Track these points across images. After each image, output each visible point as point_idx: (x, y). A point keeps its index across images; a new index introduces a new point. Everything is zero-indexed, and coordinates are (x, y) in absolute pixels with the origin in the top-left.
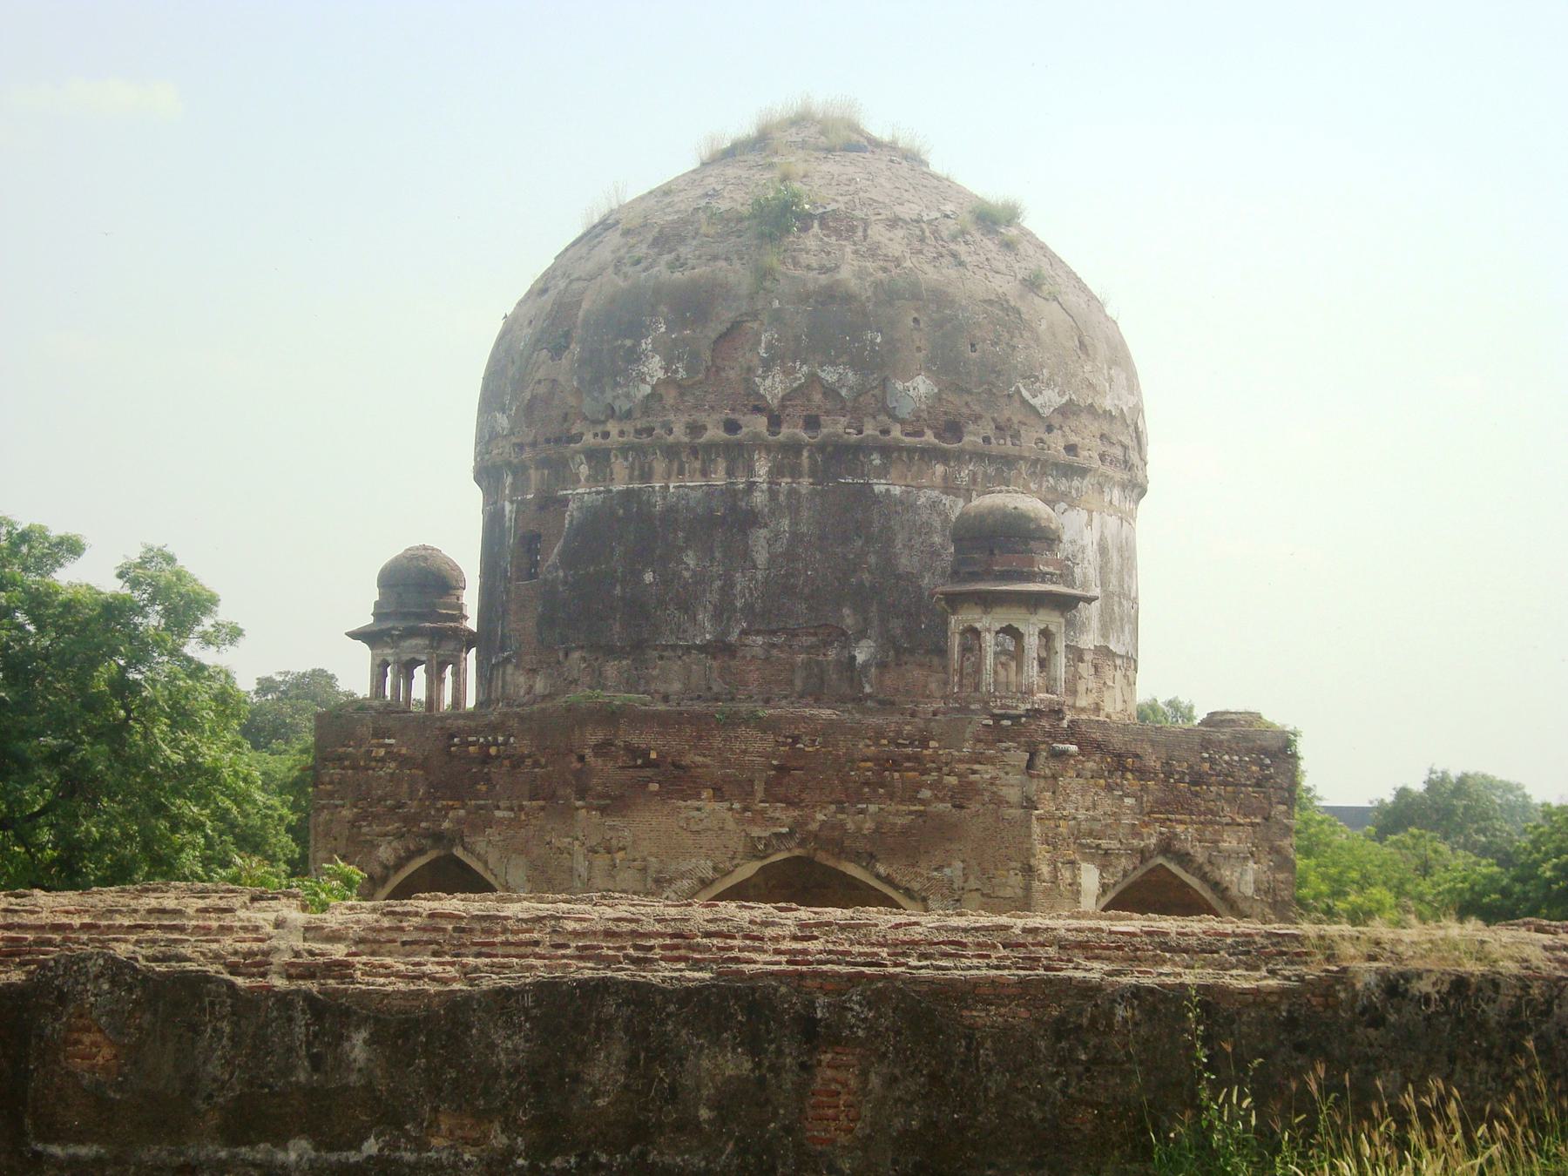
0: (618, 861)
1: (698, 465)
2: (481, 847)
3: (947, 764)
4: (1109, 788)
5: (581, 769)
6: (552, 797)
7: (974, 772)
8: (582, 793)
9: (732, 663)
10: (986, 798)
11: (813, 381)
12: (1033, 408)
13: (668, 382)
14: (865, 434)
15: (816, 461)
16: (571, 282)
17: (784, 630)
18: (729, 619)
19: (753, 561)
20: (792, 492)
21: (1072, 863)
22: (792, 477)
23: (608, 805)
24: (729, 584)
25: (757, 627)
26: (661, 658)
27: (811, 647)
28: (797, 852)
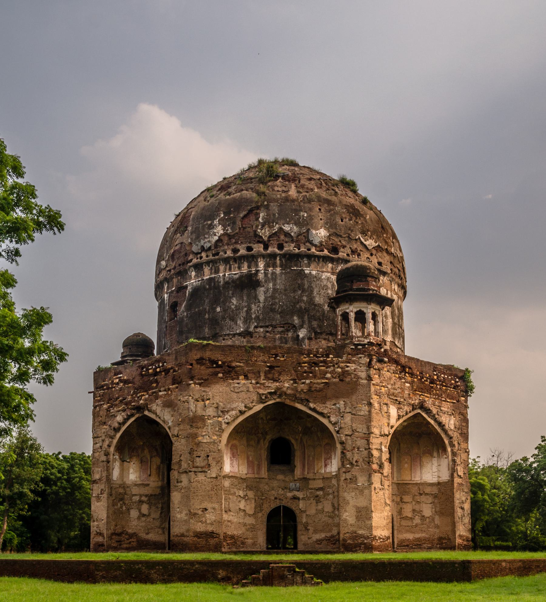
0: (207, 404)
1: (236, 266)
2: (154, 407)
3: (337, 364)
4: (400, 378)
5: (191, 369)
6: (180, 383)
7: (348, 367)
8: (192, 378)
9: (252, 339)
10: (353, 376)
11: (280, 231)
12: (365, 246)
13: (225, 234)
14: (301, 250)
15: (282, 261)
16: (188, 210)
17: (272, 325)
18: (250, 322)
19: (258, 300)
20: (273, 273)
21: (387, 404)
22: (273, 267)
23: (202, 383)
24: (249, 309)
25: (260, 324)
26: (224, 339)
27: (282, 332)
28: (278, 400)
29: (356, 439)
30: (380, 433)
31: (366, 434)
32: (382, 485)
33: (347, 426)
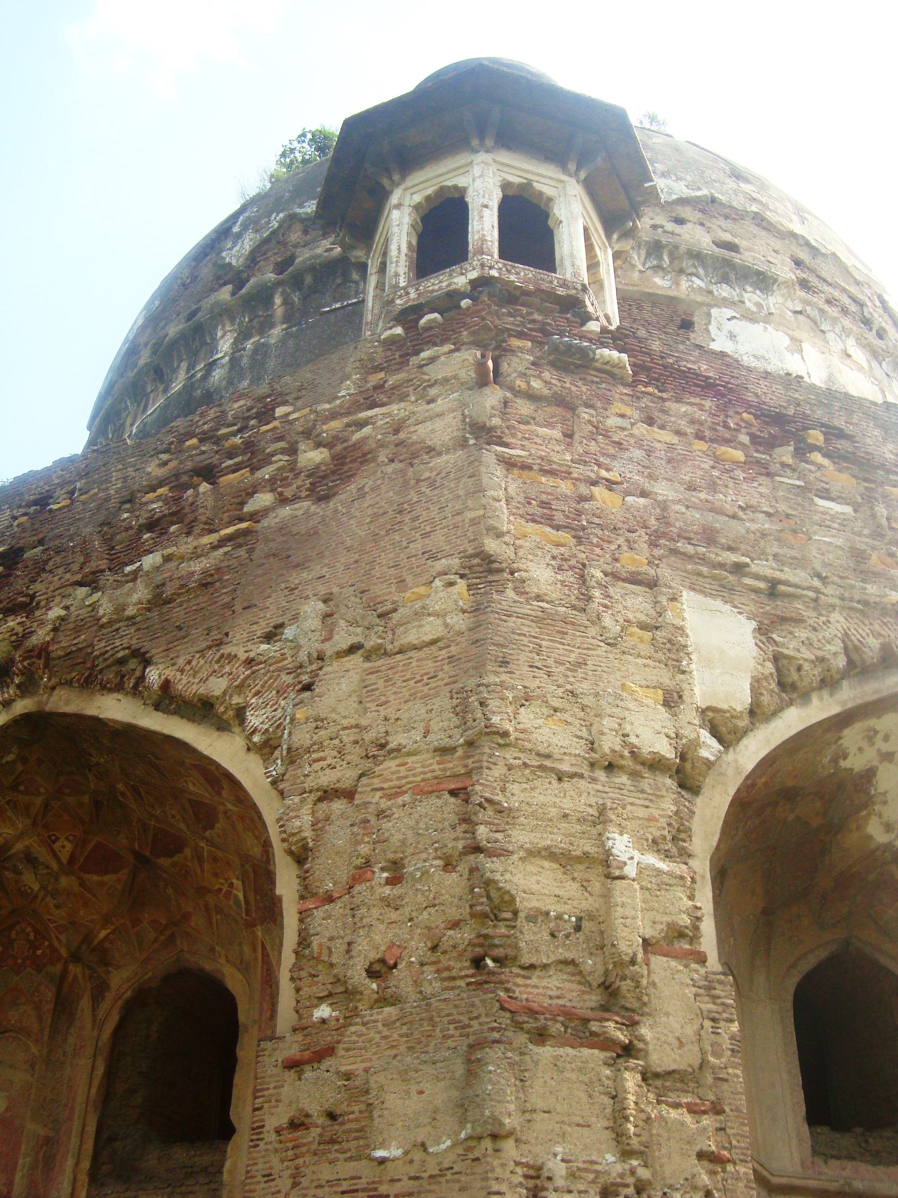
7: (361, 425)
28: (22, 706)
29: (384, 804)
30: (592, 746)
31: (444, 751)
32: (626, 1154)
33: (333, 729)
